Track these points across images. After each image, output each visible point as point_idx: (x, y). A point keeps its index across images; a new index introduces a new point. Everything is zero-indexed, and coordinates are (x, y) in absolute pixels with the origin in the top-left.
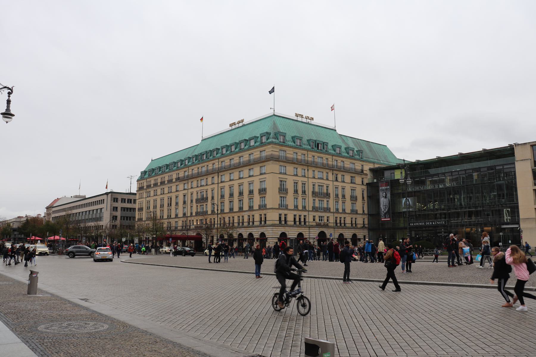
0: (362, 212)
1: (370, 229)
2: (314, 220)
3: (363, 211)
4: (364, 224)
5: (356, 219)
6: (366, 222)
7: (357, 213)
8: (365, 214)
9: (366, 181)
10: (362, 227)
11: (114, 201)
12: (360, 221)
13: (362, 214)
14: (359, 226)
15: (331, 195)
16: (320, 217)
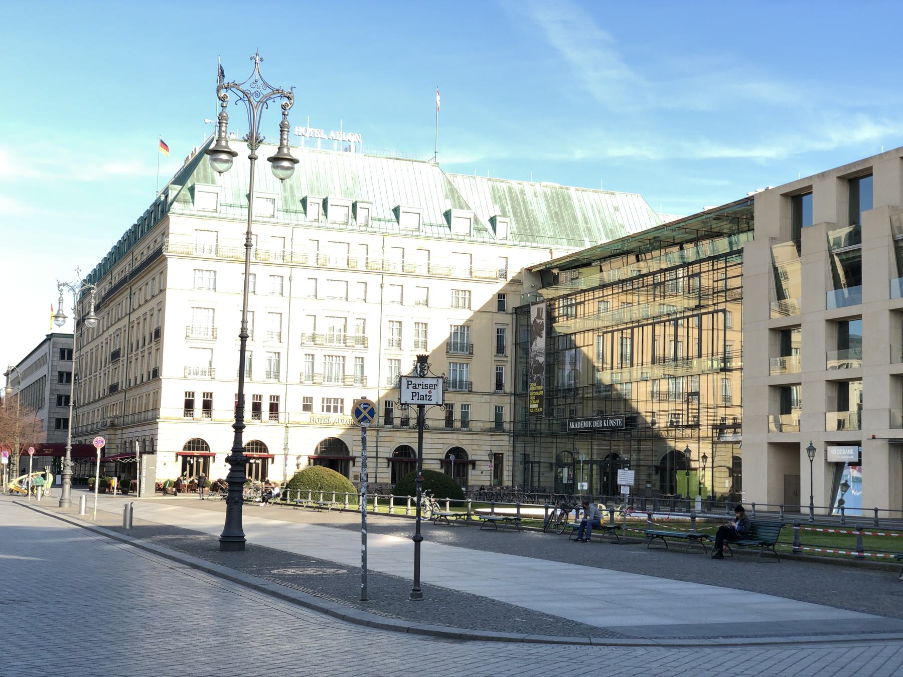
0: (493, 388)
1: (515, 436)
2: (307, 408)
3: (499, 385)
4: (499, 422)
5: (465, 407)
6: (507, 416)
7: (470, 391)
8: (505, 394)
9: (512, 302)
10: (491, 430)
11: (62, 358)
12: (482, 412)
13: (492, 394)
14: (474, 426)
15: (372, 343)
16: (329, 400)
